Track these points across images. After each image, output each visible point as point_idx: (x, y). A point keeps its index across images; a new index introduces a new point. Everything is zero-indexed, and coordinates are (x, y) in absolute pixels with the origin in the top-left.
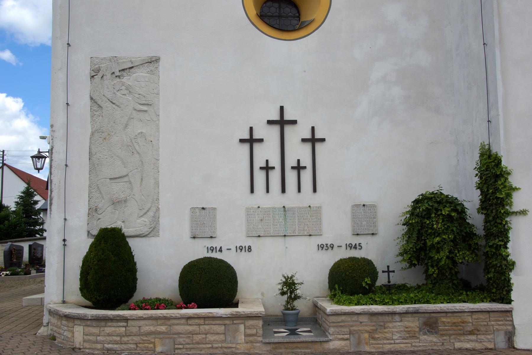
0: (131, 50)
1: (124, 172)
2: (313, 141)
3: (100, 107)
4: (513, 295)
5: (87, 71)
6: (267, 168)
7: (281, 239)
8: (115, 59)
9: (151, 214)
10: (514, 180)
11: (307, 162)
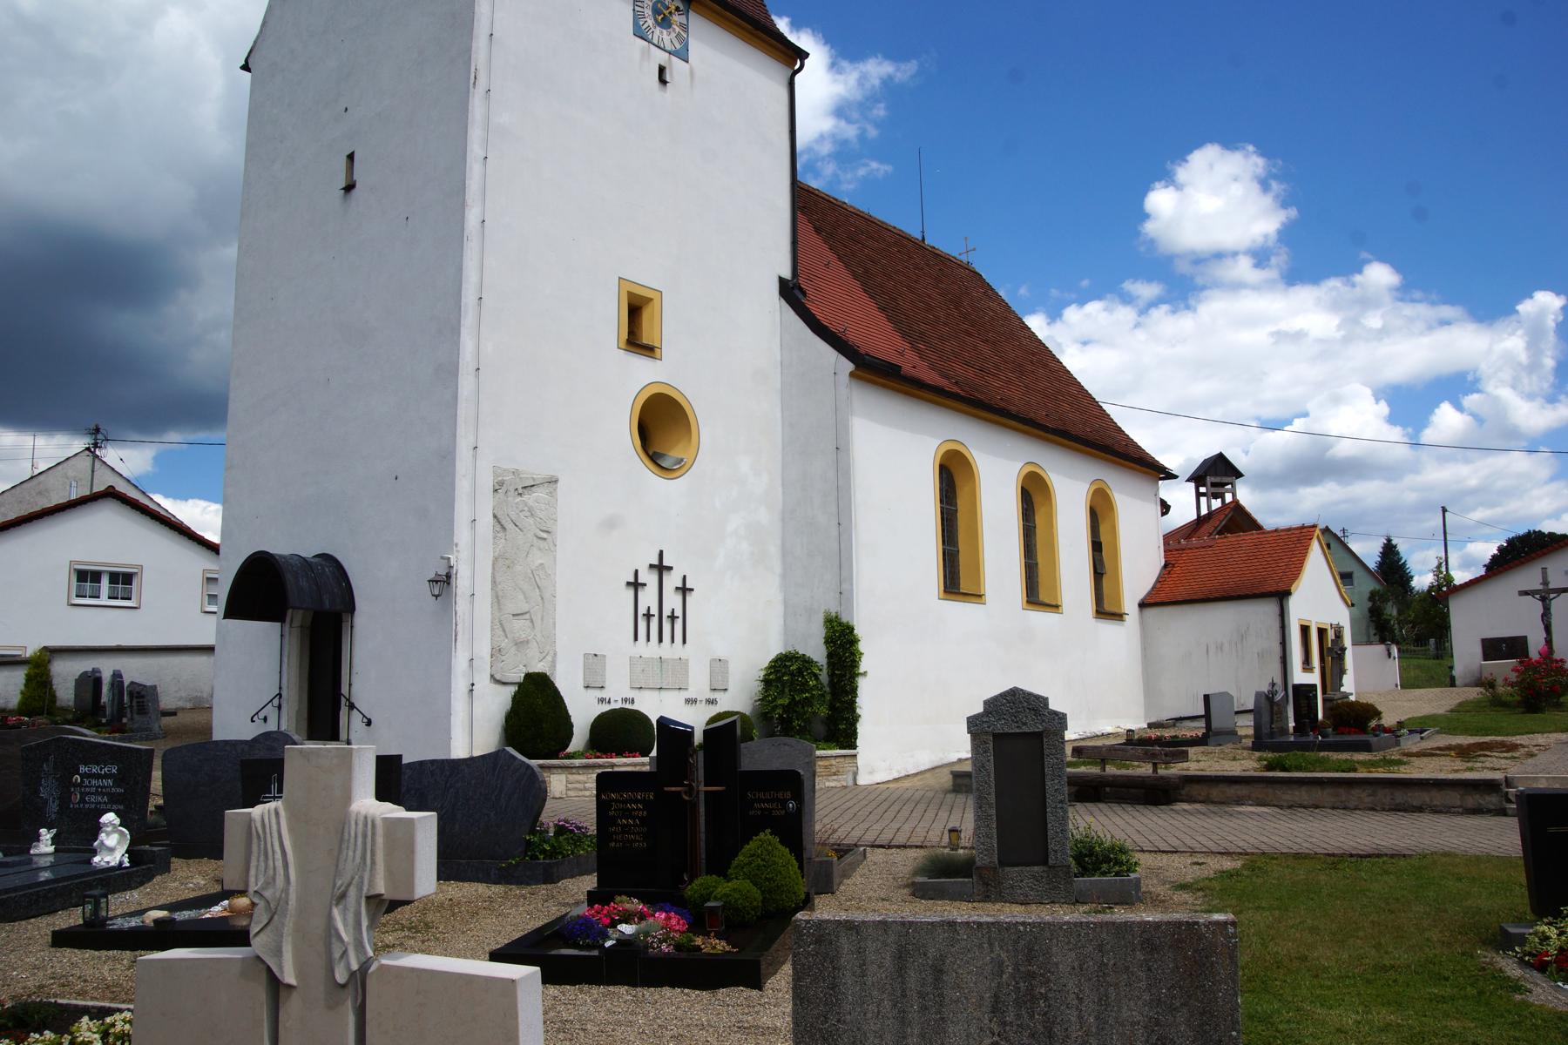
0: (535, 467)
1: (525, 608)
2: (684, 590)
3: (504, 528)
4: (859, 742)
6: (648, 616)
7: (656, 693)
8: (515, 473)
9: (549, 658)
10: (862, 647)
11: (679, 613)
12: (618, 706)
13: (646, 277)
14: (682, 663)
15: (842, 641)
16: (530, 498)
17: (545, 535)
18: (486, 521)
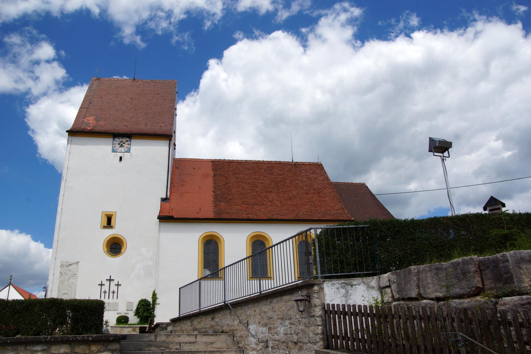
0: (71, 260)
5: (60, 265)
6: (105, 292)
11: (116, 291)
12: (124, 315)
13: (109, 209)
14: (117, 304)
15: (154, 295)
16: (70, 267)
17: (75, 275)
18: (57, 274)
